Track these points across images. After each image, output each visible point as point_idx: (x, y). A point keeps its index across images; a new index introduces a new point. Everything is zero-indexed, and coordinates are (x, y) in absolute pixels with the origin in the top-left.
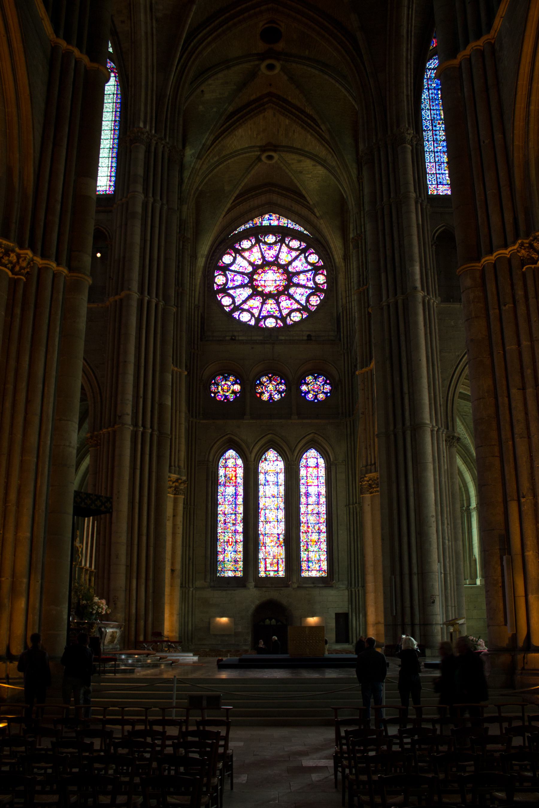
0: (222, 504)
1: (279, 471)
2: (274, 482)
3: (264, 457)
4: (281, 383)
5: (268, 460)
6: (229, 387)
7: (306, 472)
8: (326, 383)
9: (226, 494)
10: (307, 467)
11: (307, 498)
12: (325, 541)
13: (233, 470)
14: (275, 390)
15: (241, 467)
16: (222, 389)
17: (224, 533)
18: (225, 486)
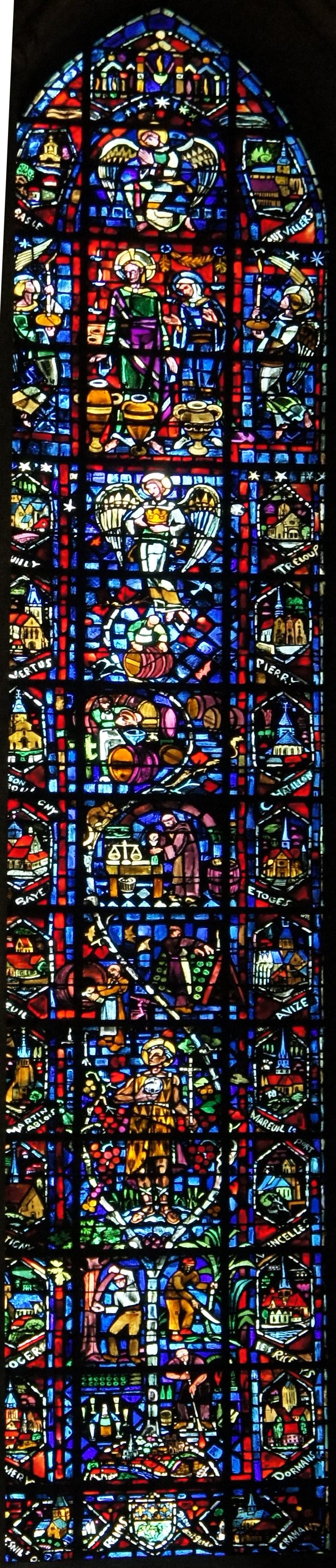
12: (309, 1134)
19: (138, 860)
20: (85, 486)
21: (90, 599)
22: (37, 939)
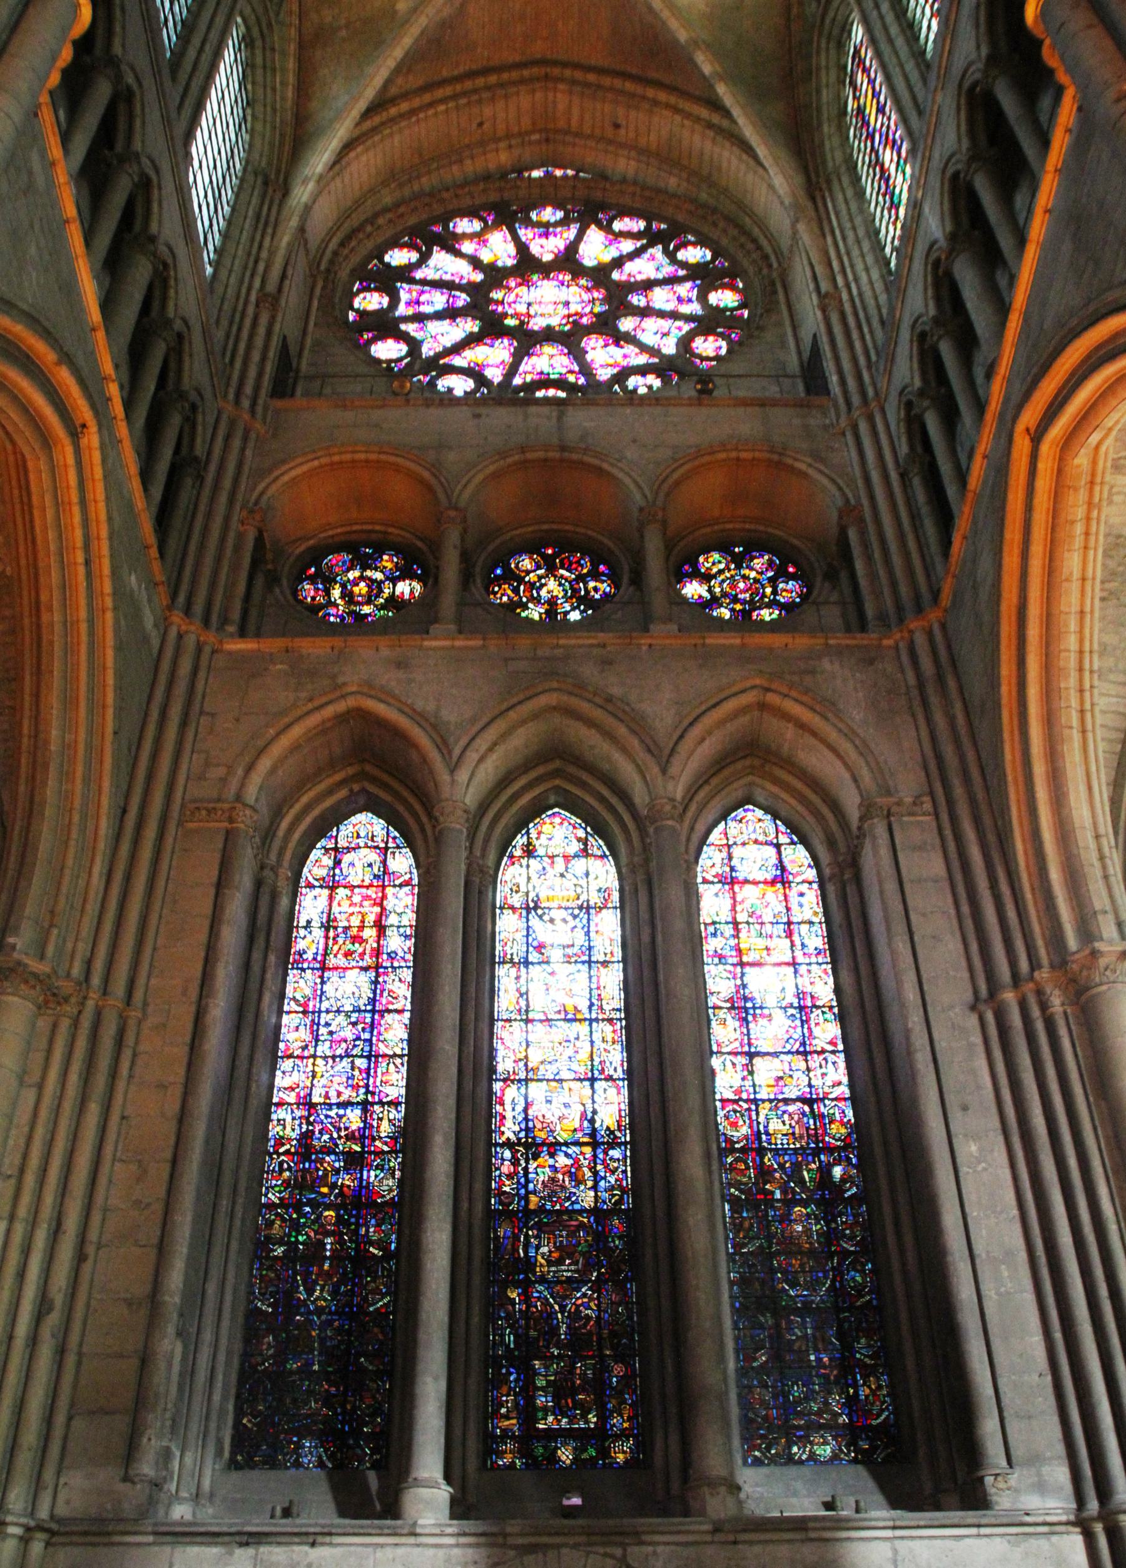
0: (301, 1058)
1: (595, 899)
2: (570, 951)
3: (520, 840)
4: (595, 575)
5: (541, 851)
6: (375, 587)
7: (728, 903)
8: (781, 574)
9: (325, 1005)
10: (730, 881)
11: (744, 1021)
13: (368, 897)
14: (571, 597)
15: (407, 883)
16: (347, 595)
17: (298, 1207)
18: (324, 968)
19: (780, 1126)
20: (743, 974)
21: (750, 1018)
22: (746, 1164)
